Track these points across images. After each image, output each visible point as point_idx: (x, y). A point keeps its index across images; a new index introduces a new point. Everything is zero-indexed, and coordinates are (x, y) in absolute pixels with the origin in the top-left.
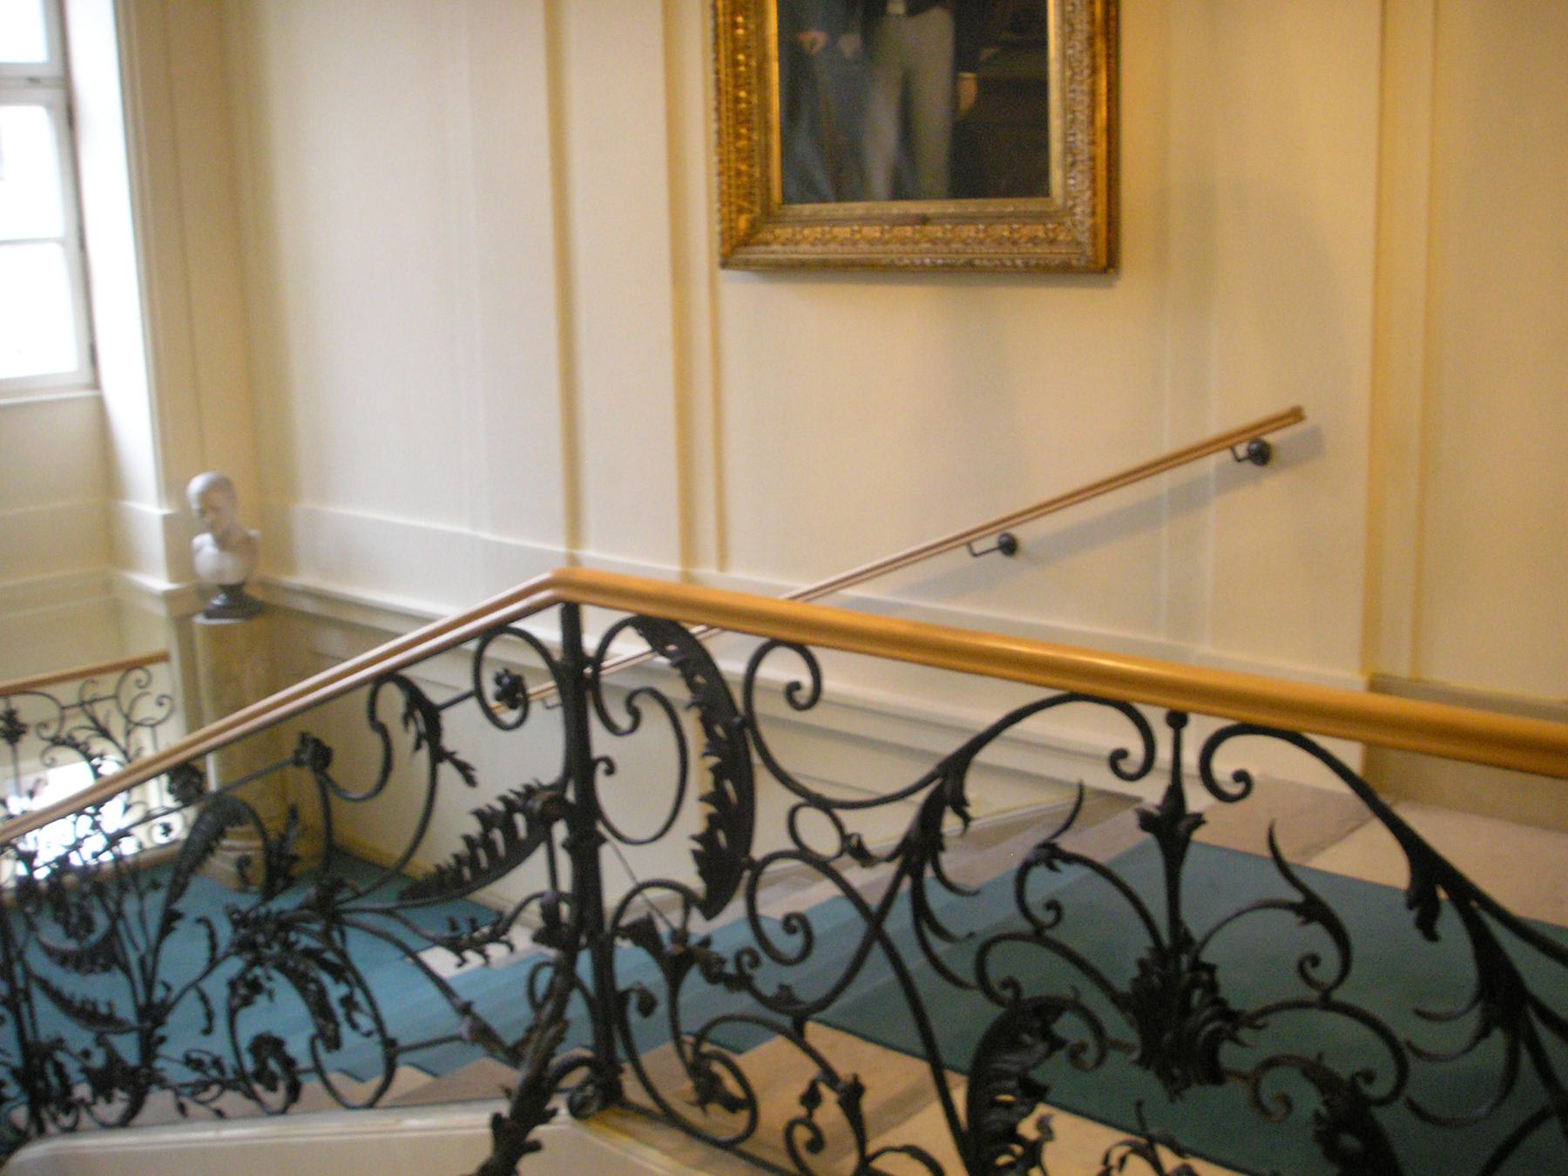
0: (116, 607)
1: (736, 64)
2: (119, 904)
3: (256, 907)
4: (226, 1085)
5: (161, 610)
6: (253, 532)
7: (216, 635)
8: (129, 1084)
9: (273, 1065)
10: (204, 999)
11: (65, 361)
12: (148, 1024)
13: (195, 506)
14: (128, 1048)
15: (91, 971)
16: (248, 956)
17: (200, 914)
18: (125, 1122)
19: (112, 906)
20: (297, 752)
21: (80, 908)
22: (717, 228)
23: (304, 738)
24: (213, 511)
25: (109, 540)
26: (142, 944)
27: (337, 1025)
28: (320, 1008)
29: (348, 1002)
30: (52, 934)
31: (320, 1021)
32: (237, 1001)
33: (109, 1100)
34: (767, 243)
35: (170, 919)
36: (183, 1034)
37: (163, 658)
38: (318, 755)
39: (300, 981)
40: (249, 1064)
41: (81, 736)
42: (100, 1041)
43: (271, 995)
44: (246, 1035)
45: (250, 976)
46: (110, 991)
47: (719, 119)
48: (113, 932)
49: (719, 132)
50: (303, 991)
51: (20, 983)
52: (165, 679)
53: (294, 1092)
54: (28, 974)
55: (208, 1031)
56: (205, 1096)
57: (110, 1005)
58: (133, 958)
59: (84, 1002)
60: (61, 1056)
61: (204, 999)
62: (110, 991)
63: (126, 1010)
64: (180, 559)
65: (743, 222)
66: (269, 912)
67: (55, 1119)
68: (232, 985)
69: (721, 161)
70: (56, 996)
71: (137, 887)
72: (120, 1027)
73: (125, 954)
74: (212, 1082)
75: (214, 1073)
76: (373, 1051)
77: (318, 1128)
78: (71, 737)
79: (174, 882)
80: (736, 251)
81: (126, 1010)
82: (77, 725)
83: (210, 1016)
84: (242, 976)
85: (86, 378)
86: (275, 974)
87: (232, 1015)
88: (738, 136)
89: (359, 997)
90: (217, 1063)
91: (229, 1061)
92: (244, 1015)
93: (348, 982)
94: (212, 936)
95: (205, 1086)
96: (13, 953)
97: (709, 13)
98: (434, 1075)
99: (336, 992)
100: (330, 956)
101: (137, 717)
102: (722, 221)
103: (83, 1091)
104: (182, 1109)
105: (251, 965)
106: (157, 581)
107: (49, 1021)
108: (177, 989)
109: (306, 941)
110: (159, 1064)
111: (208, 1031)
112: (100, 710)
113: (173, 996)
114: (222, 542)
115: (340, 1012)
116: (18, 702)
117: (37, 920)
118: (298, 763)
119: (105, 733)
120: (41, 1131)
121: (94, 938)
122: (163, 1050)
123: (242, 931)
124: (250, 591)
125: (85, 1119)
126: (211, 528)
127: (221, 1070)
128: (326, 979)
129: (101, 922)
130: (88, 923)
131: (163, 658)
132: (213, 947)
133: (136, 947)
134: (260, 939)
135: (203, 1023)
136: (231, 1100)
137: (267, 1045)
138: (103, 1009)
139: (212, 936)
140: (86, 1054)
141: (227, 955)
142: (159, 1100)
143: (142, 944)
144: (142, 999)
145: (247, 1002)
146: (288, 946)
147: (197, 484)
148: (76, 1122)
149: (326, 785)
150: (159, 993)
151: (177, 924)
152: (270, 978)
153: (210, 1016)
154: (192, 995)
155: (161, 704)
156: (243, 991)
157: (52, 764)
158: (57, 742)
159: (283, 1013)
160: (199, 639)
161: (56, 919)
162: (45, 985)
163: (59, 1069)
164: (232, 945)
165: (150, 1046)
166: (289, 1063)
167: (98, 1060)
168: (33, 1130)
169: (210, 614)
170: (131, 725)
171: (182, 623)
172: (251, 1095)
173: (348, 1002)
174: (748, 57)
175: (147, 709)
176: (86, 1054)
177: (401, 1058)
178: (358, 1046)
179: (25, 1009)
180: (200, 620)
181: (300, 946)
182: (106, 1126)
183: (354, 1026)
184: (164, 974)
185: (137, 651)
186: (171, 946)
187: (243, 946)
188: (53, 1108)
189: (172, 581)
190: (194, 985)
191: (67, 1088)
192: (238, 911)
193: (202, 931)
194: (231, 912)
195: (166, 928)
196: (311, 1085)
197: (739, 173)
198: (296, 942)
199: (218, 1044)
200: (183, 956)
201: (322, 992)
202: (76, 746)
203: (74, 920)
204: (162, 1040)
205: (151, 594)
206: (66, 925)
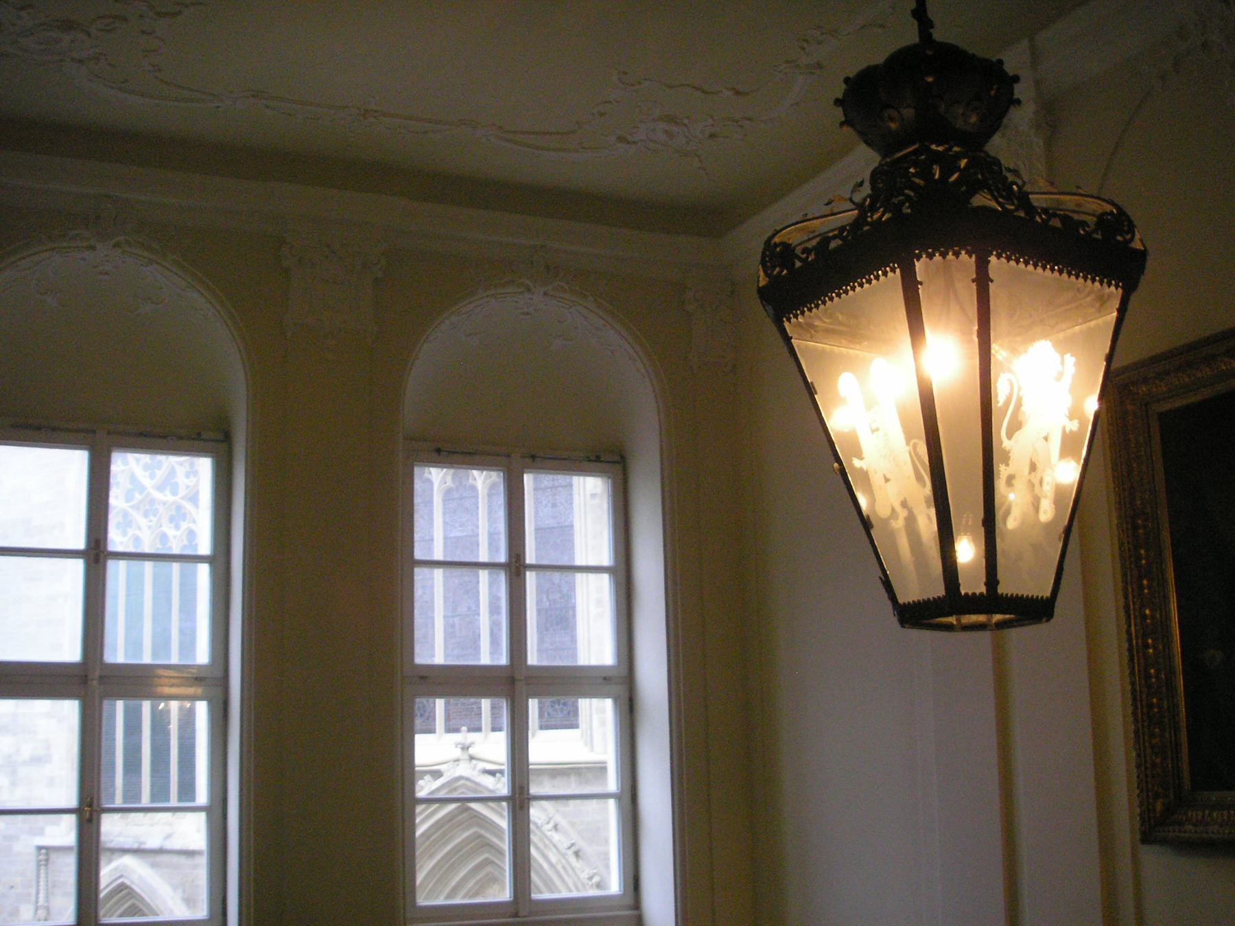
1: (1148, 676)
11: (614, 886)
22: (1138, 810)
34: (1180, 824)
47: (1136, 721)
49: (1136, 732)
65: (1159, 806)
69: (1139, 755)
80: (1153, 830)
85: (629, 900)
88: (1152, 735)
97: (1124, 636)
102: (1141, 805)
174: (1158, 671)
197: (1154, 765)
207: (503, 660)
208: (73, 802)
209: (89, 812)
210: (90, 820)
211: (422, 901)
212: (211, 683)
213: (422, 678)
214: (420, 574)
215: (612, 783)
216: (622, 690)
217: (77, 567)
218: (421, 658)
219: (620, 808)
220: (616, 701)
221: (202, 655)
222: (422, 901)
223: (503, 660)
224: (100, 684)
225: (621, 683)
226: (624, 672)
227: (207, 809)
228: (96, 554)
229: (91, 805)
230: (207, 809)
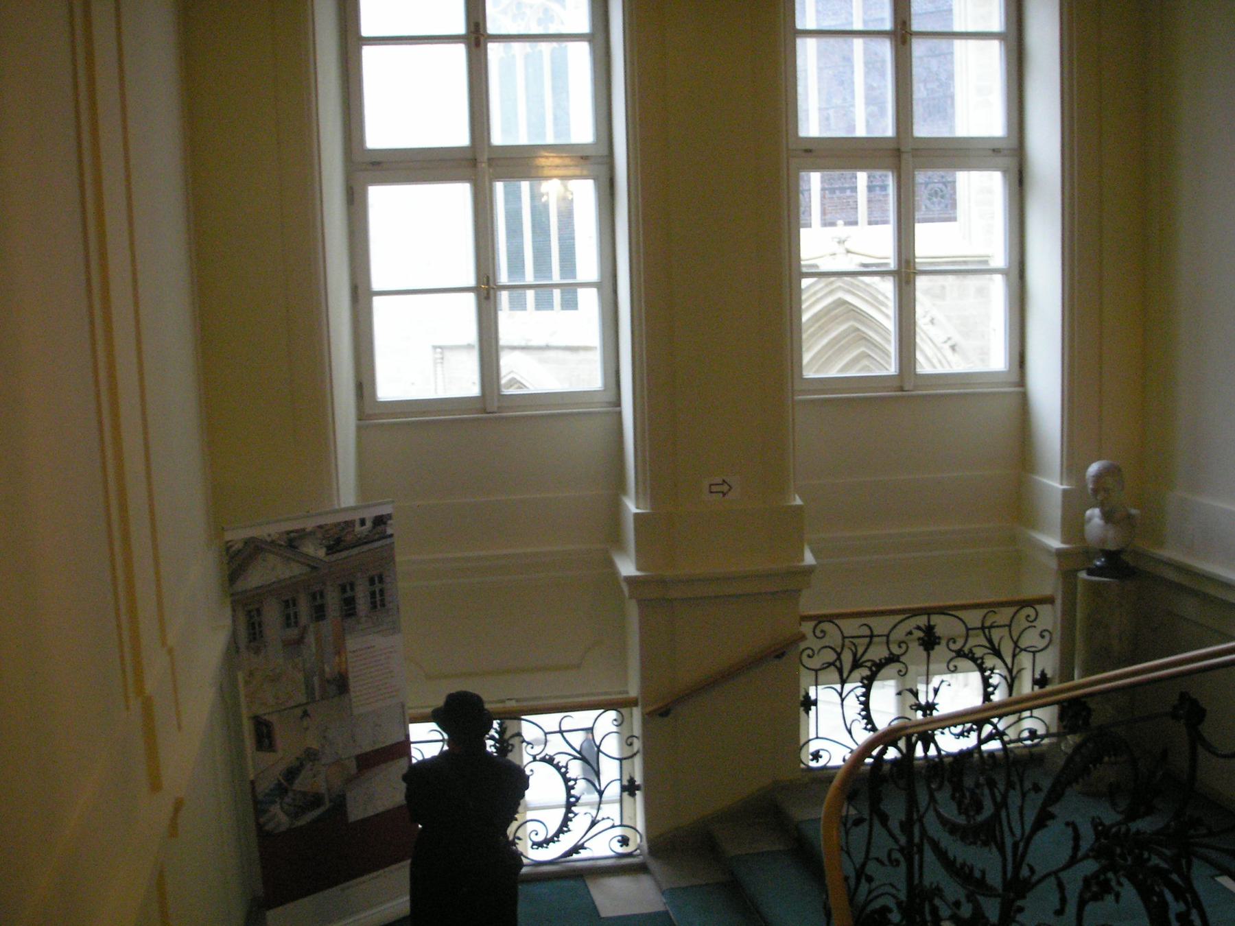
0: (1017, 554)
2: (1005, 797)
3: (1119, 824)
5: (1053, 564)
6: (1133, 511)
7: (1094, 589)
10: (1061, 886)
11: (997, 360)
13: (1091, 486)
15: (975, 843)
17: (1070, 819)
19: (999, 799)
20: (1175, 707)
21: (973, 792)
23: (1184, 696)
24: (1102, 491)
25: (1019, 503)
26: (1018, 832)
30: (950, 811)
32: (1087, 895)
35: (1043, 820)
37: (1050, 600)
38: (1191, 711)
39: (1145, 893)
41: (978, 652)
42: (970, 898)
43: (1117, 896)
45: (1102, 877)
46: (987, 862)
48: (996, 816)
50: (1146, 899)
51: (917, 840)
52: (1049, 617)
54: (923, 832)
55: (1060, 912)
57: (983, 873)
58: (1009, 842)
59: (964, 865)
60: (937, 902)
61: (1061, 886)
62: (987, 862)
63: (995, 879)
64: (1073, 524)
66: (1128, 830)
68: (1087, 881)
70: (942, 855)
71: (1022, 786)
72: (989, 891)
78: (971, 651)
79: (1053, 789)
81: (995, 879)
82: (978, 640)
83: (1063, 900)
84: (1096, 875)
85: (1014, 377)
86: (1124, 880)
92: (1090, 907)
93: (1186, 902)
94: (1077, 838)
96: (915, 817)
99: (1175, 907)
100: (1175, 877)
101: (1023, 644)
105: (1104, 870)
106: (1055, 543)
107: (934, 874)
108: (1041, 871)
109: (1155, 860)
111: (1060, 912)
112: (996, 635)
113: (1035, 878)
114: (1107, 517)
116: (935, 619)
117: (938, 796)
118: (1175, 716)
119: (997, 653)
121: (980, 818)
122: (1019, 917)
124: (1124, 557)
126: (1101, 505)
128: (1169, 897)
129: (988, 810)
130: (979, 808)
131: (1050, 600)
132: (1076, 848)
133: (1013, 834)
134: (1118, 850)
135: (1058, 907)
138: (977, 874)
139: (1077, 838)
140: (957, 904)
141: (1086, 857)
143: (1018, 832)
144: (1009, 875)
145: (1097, 897)
147: (1094, 468)
149: (1196, 739)
150: (1025, 872)
151: (1049, 823)
152: (1120, 884)
153: (1063, 900)
155: (1043, 637)
156: (1095, 889)
157: (955, 670)
158: (960, 654)
160: (1079, 589)
161: (953, 797)
162: (935, 846)
163: (935, 911)
164: (1092, 849)
167: (966, 911)
169: (1091, 572)
170: (1017, 650)
171: (1068, 576)
175: (1031, 639)
176: (957, 904)
179: (917, 857)
180: (1083, 575)
181: (1151, 863)
184: (1029, 859)
185: (1028, 593)
186: (1041, 837)
187: (1097, 853)
189: (1063, 542)
190: (1055, 873)
192: (1101, 824)
193: (1070, 830)
194: (1096, 824)
195: (1041, 822)
198: (1149, 859)
200: (1049, 848)
201: (1164, 905)
202: (974, 660)
203: (967, 801)
205: (1047, 550)
206: (960, 804)
207: (889, 132)
208: (471, 281)
209: (486, 291)
210: (487, 298)
211: (809, 374)
212: (594, 161)
213: (808, 151)
214: (799, 41)
215: (999, 258)
216: (1012, 162)
217: (460, 50)
218: (803, 133)
219: (1009, 285)
220: (1005, 172)
221: (583, 132)
222: (809, 374)
223: (889, 132)
224: (490, 165)
225: (1011, 156)
226: (1014, 143)
227: (598, 285)
228: (476, 37)
229: (488, 283)
230: (598, 285)
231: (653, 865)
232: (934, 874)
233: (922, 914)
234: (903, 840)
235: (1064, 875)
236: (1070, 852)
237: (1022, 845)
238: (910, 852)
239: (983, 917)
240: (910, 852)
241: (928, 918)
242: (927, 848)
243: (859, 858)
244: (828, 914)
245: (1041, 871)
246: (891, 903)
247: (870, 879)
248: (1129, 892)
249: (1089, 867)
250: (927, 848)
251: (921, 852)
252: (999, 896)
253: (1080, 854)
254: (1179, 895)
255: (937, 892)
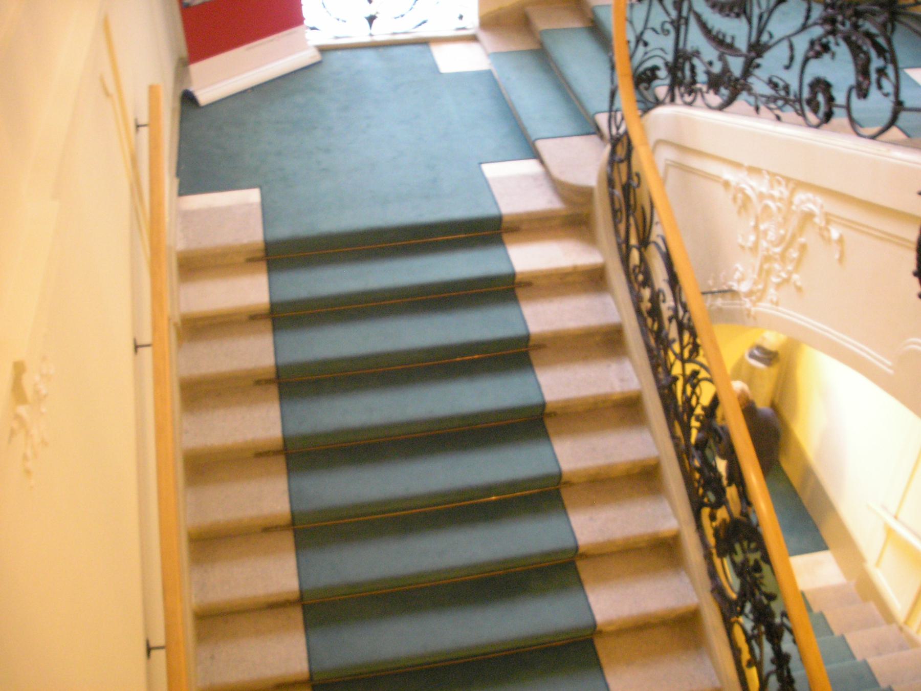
4: (786, 101)
8: (730, 87)
9: (821, 98)
10: (791, 47)
12: (753, 54)
14: (736, 65)
15: (728, 15)
16: (828, 27)
18: (721, 108)
27: (869, 84)
28: (863, 71)
29: (881, 72)
31: (861, 79)
32: (811, 54)
33: (717, 92)
36: (772, 63)
39: (855, 49)
40: (806, 94)
42: (721, 58)
43: (833, 55)
44: (808, 79)
45: (824, 40)
51: (684, 13)
53: (828, 116)
54: (690, 8)
55: (787, 67)
56: (772, 106)
57: (733, 38)
58: (756, 12)
59: (718, 33)
60: (696, 61)
61: (791, 47)
62: (737, 30)
67: (682, 96)
68: (812, 43)
73: (751, 10)
74: (781, 98)
75: (782, 93)
76: (888, 105)
77: (836, 141)
81: (742, 44)
83: (792, 59)
84: (820, 39)
87: (806, 60)
89: (890, 70)
90: (787, 88)
91: (794, 87)
93: (885, 59)
95: (775, 100)
98: (908, 136)
99: (876, 63)
100: (881, 41)
103: (701, 85)
104: (757, 109)
107: (695, 38)
108: (777, 36)
109: (868, 26)
110: (751, 80)
111: (787, 67)
115: (874, 76)
120: (673, 100)
122: (757, 72)
123: (830, 11)
125: (699, 101)
127: (788, 93)
128: (873, 53)
132: (807, 17)
133: (759, 6)
134: (840, 18)
135: (786, 62)
136: (789, 113)
137: (822, 85)
138: (728, 40)
140: (711, 63)
141: (815, 24)
142: (742, 102)
144: (754, 38)
145: (818, 55)
146: (856, 27)
148: (694, 100)
150: (765, 38)
152: (837, 44)
153: (792, 59)
154: (785, 45)
156: (818, 48)
159: (839, 70)
162: (698, 17)
163: (693, 68)
164: (820, 18)
165: (749, 67)
166: (830, 99)
167: (717, 68)
168: (668, 100)
172: (802, 114)
173: (881, 72)
176: (711, 63)
177: (903, 116)
178: (877, 104)
179: (683, 28)
182: (710, 107)
183: (880, 87)
188: (682, 89)
190: (788, 37)
191: (694, 82)
196: (840, 118)
199: (791, 78)
201: (868, 60)
204: (758, 66)
231: (482, 36)
232: (695, 38)
233: (683, 70)
234: (674, 14)
235: (795, 40)
236: (800, 21)
237: (765, 16)
238: (679, 24)
239: (729, 71)
240: (679, 24)
241: (688, 73)
242: (693, 22)
243: (639, 27)
244: (613, 68)
245: (777, 36)
246: (659, 62)
247: (646, 44)
248: (842, 51)
249: (817, 31)
250: (693, 22)
251: (687, 23)
252: (741, 56)
253: (810, 21)
254: (881, 51)
255: (697, 54)
